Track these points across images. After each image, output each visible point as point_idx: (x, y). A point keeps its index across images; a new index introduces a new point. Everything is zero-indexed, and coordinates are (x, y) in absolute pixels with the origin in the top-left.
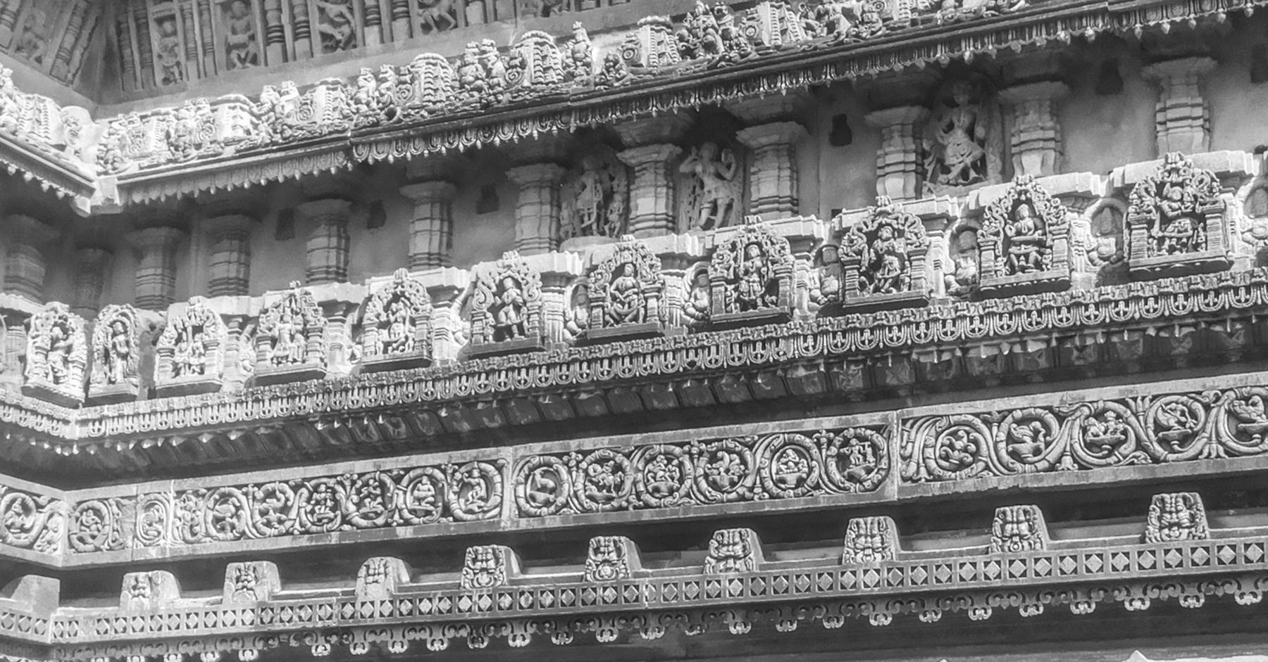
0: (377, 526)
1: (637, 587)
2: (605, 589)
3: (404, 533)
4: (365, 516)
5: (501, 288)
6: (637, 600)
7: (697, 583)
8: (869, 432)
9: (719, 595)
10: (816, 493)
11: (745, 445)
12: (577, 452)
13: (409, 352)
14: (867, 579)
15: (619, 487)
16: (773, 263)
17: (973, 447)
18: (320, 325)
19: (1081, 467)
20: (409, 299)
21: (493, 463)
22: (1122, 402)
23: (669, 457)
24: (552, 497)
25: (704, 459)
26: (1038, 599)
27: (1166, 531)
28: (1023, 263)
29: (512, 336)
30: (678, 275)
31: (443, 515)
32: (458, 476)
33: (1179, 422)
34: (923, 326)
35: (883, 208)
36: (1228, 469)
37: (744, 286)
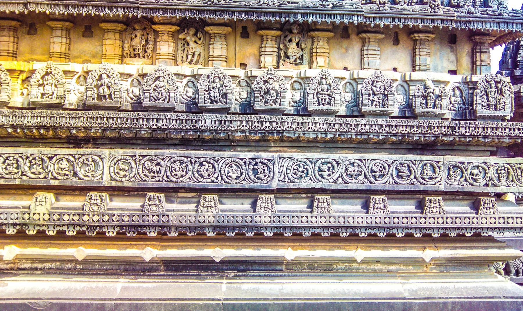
0: (40, 179)
1: (168, 216)
2: (153, 216)
3: (53, 183)
4: (33, 173)
5: (100, 78)
6: (168, 221)
7: (195, 216)
8: (266, 161)
9: (204, 222)
10: (244, 183)
11: (215, 161)
12: (140, 156)
13: (54, 100)
14: (265, 219)
15: (159, 172)
16: (225, 86)
17: (305, 171)
18: (8, 81)
19: (345, 183)
20: (54, 76)
21: (99, 156)
22: (360, 160)
23: (182, 163)
24: (127, 174)
25: (196, 165)
26: (328, 230)
27: (376, 210)
28: (323, 102)
29: (106, 99)
30: (180, 82)
31: (73, 176)
32: (81, 160)
33: (379, 170)
34: (290, 123)
35: (271, 72)
36: (395, 189)
37: (212, 94)
